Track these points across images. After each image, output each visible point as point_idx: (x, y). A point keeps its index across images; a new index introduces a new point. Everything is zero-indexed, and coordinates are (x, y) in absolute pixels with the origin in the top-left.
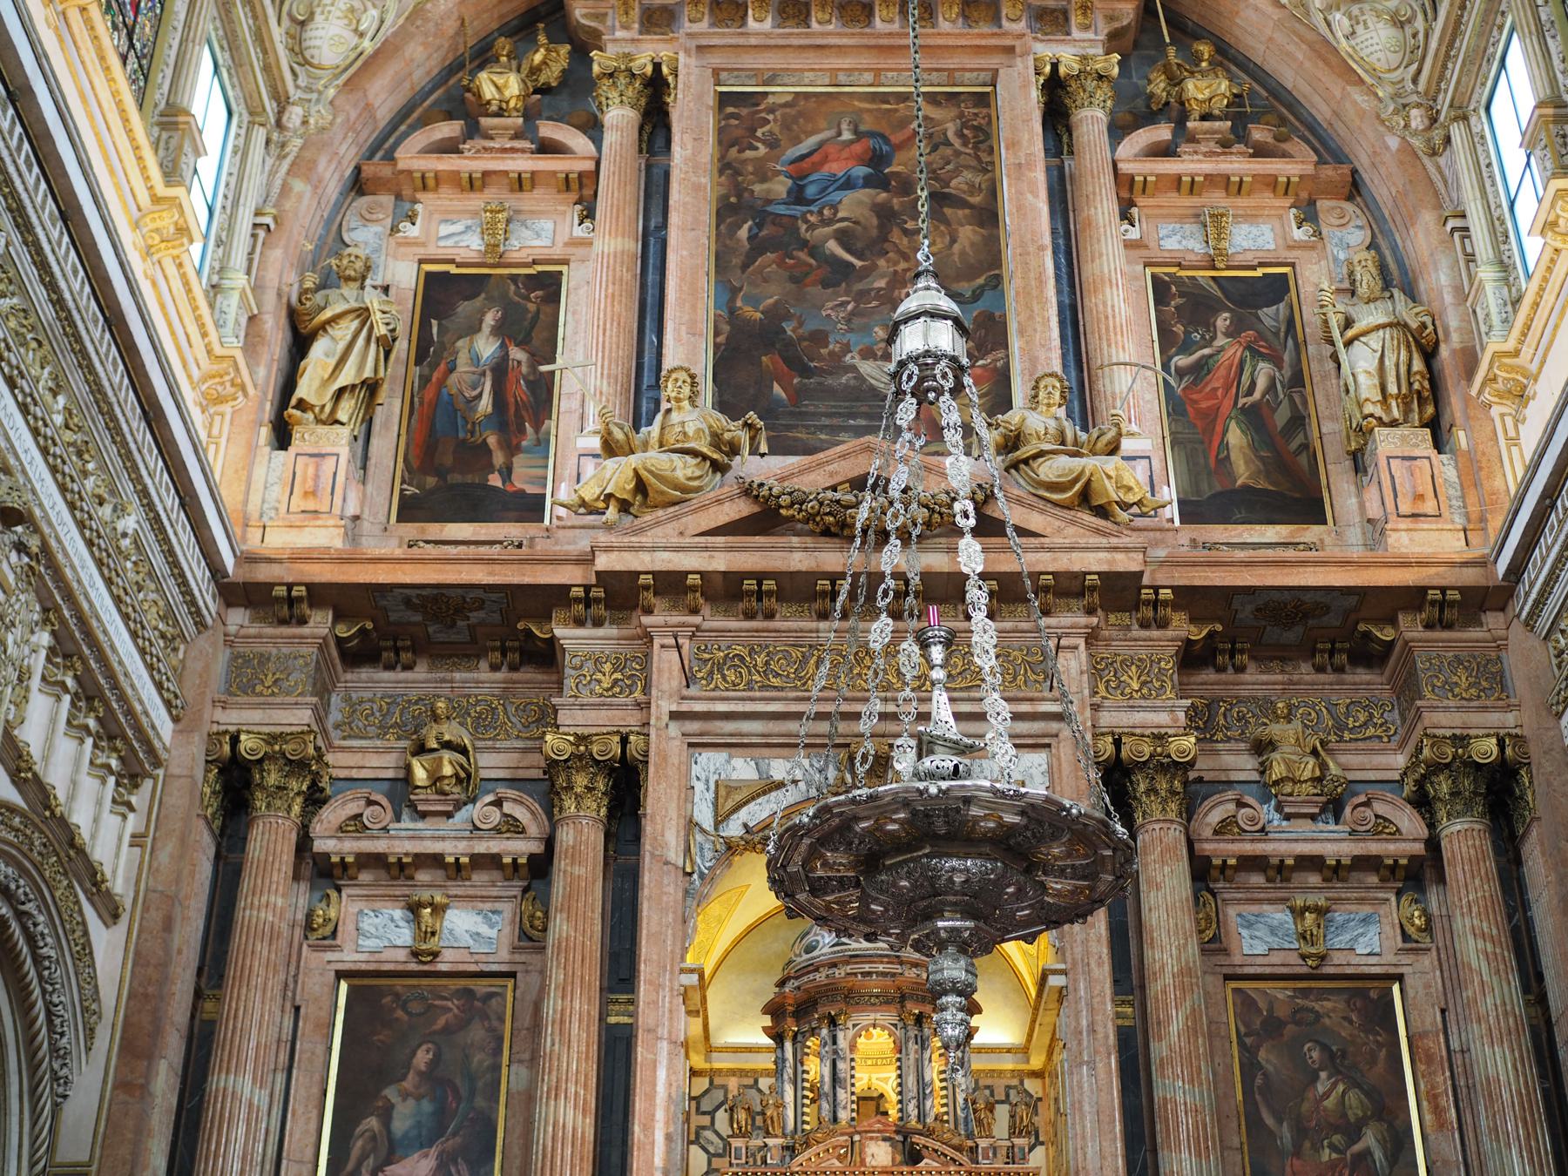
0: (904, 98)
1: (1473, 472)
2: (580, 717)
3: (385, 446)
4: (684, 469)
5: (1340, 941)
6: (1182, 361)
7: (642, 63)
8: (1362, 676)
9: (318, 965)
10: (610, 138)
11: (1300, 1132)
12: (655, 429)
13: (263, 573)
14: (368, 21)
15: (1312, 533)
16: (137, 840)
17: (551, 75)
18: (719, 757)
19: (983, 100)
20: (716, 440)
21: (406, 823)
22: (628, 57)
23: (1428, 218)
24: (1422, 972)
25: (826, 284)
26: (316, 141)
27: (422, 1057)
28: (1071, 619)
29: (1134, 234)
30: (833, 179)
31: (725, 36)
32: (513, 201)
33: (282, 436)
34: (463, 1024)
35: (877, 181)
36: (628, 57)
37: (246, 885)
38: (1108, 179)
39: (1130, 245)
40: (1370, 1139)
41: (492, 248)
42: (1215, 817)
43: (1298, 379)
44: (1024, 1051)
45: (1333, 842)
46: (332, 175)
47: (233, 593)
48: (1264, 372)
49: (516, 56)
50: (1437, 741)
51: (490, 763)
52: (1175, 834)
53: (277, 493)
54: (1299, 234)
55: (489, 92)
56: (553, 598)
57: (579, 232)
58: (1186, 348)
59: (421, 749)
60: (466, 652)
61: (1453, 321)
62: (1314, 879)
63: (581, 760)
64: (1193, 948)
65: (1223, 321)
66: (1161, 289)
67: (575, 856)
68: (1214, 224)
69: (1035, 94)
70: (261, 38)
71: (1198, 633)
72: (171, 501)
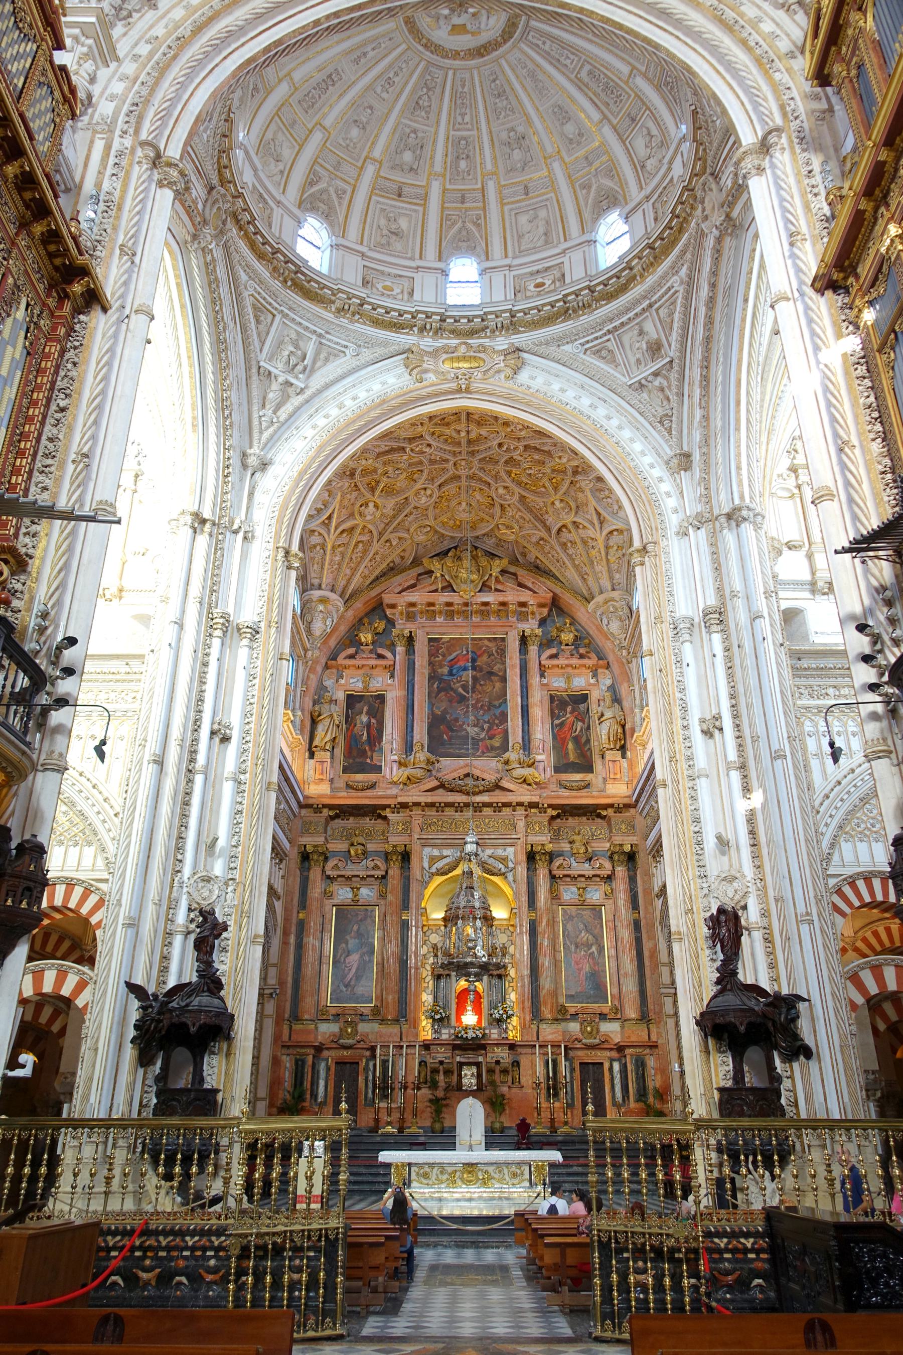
0: (481, 639)
1: (631, 766)
2: (394, 839)
3: (339, 751)
4: (419, 773)
5: (588, 896)
6: (557, 722)
7: (406, 633)
8: (599, 820)
9: (328, 903)
10: (398, 657)
11: (577, 947)
12: (412, 757)
13: (310, 801)
14: (329, 622)
15: (589, 777)
16: (283, 877)
17: (380, 630)
18: (429, 849)
19: (503, 639)
20: (428, 762)
21: (350, 866)
22: (402, 630)
23: (626, 685)
24: (609, 903)
25: (459, 702)
26: (316, 661)
27: (355, 928)
28: (521, 811)
29: (545, 681)
30: (460, 667)
31: (431, 623)
32: (370, 672)
33: (312, 756)
34: (365, 918)
35: (474, 668)
36: (402, 630)
37: (310, 887)
38: (537, 671)
39: (543, 685)
40: (594, 949)
41: (366, 688)
42: (557, 864)
43: (589, 728)
44: (509, 920)
45: (586, 869)
46: (319, 669)
47: (301, 806)
48: (580, 724)
49: (370, 624)
50: (615, 845)
51: (371, 847)
52: (547, 871)
53: (312, 772)
54: (592, 681)
55: (363, 640)
56: (385, 807)
57: (389, 682)
58: (558, 718)
59: (352, 845)
60: (364, 815)
61: (628, 719)
62: (583, 879)
63: (394, 852)
64: (549, 903)
65: (569, 709)
66: (552, 698)
67: (393, 877)
68: (568, 679)
69: (517, 643)
70: (301, 640)
71: (554, 813)
72: (290, 795)
